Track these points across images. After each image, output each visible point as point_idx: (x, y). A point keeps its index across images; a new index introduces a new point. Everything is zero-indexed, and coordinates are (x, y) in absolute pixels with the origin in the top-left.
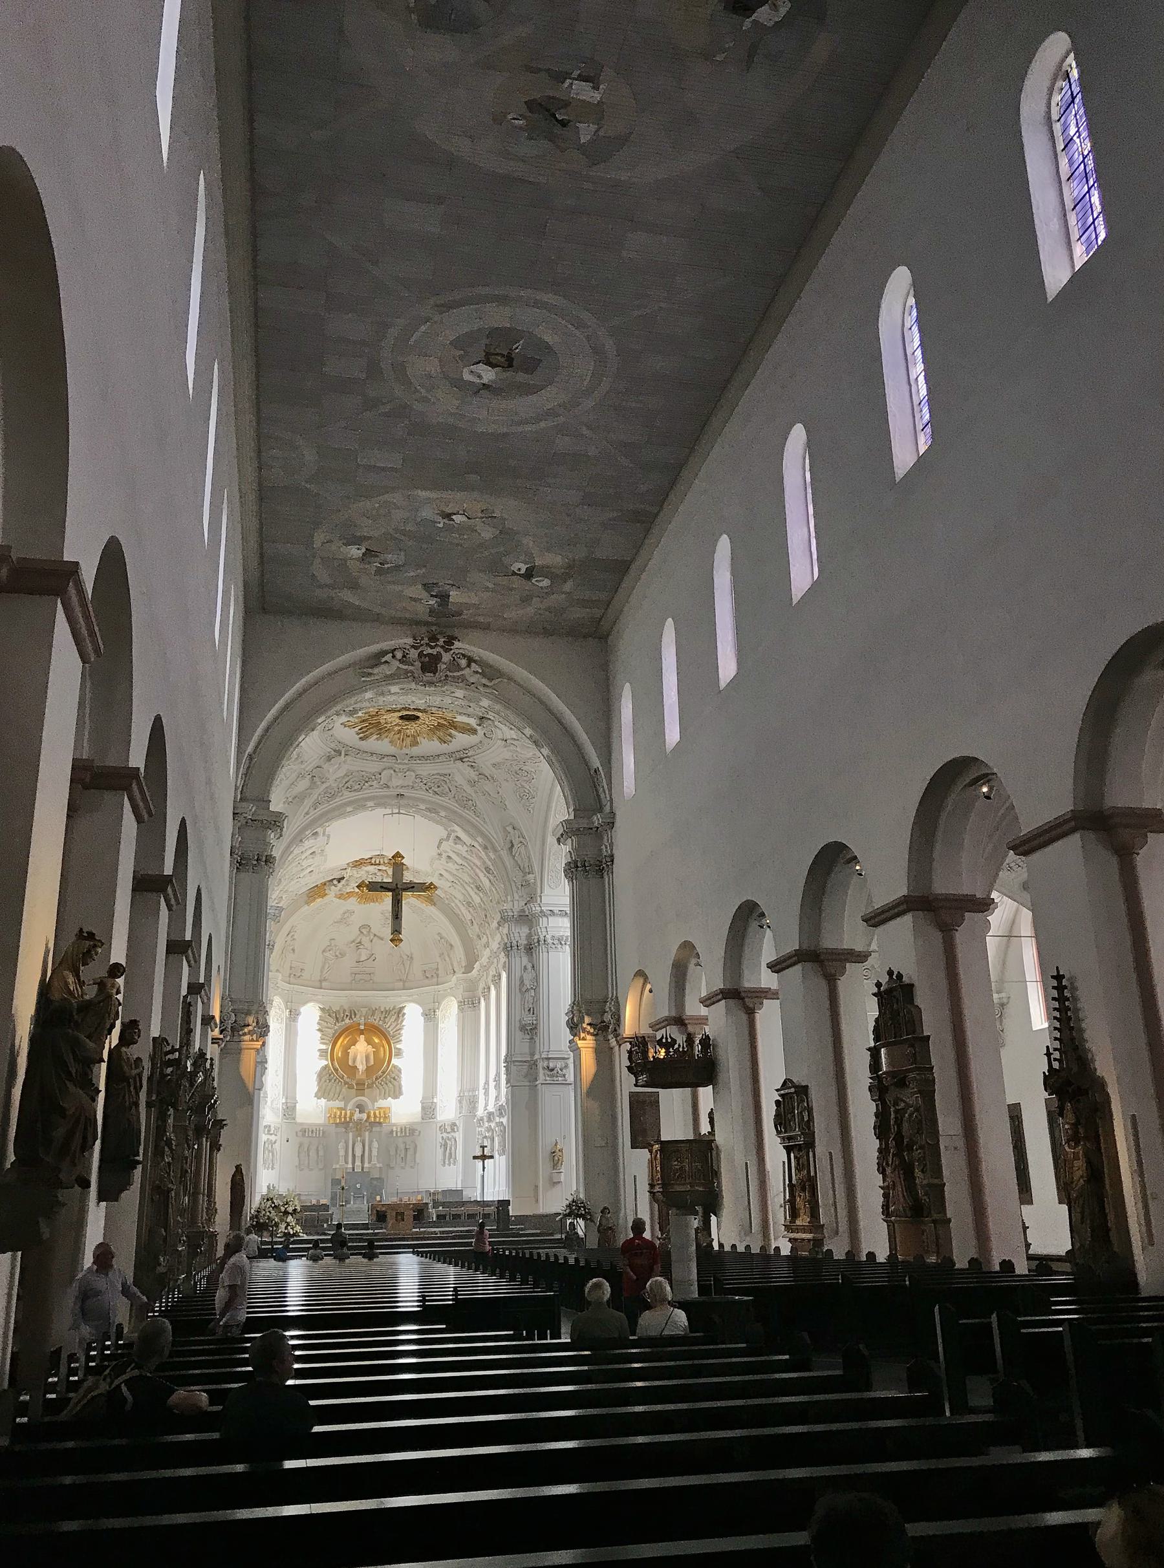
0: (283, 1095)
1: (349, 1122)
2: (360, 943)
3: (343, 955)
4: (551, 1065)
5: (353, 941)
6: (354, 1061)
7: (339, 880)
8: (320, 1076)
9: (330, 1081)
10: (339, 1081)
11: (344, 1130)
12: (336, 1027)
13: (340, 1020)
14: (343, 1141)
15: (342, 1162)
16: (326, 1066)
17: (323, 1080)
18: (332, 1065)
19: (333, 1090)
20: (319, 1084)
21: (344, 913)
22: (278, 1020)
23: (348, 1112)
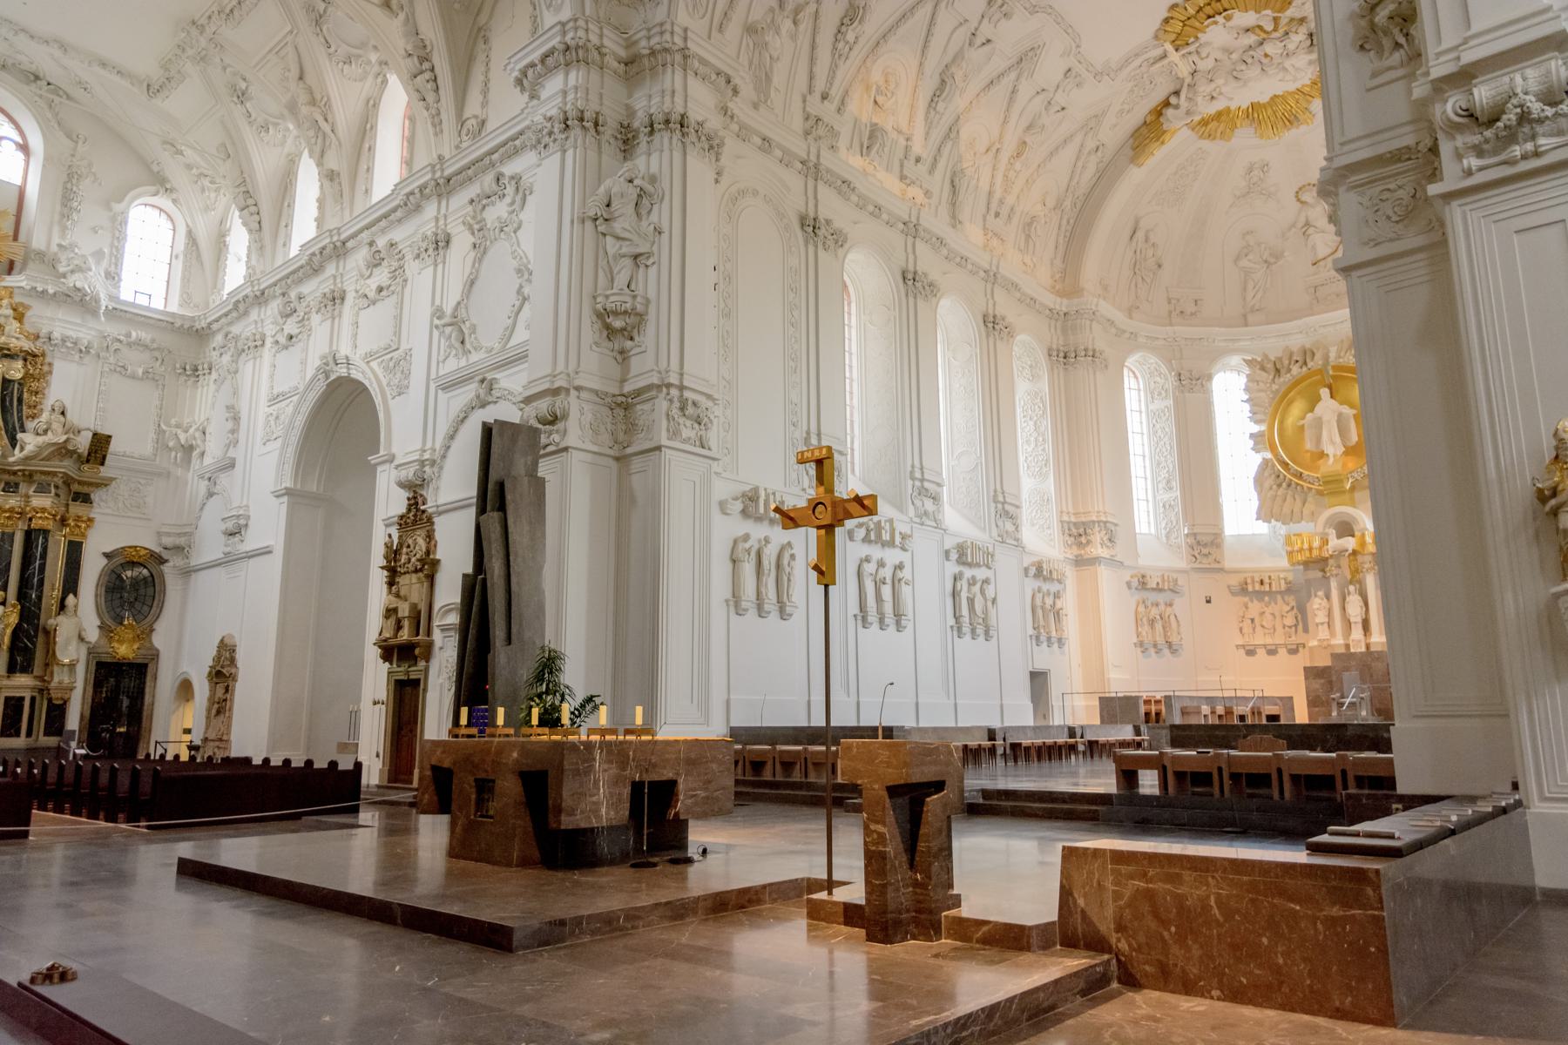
0: (1185, 520)
1: (1325, 560)
2: (1307, 224)
3: (1278, 256)
4: (1483, 94)
5: (1294, 225)
6: (1318, 440)
7: (1177, 93)
8: (1259, 481)
9: (1279, 486)
10: (1297, 484)
11: (1320, 574)
12: (1275, 387)
13: (1283, 371)
14: (1320, 593)
15: (1323, 633)
16: (1265, 462)
17: (1267, 485)
18: (1276, 455)
19: (1289, 499)
20: (1259, 494)
21: (1250, 170)
22: (1160, 394)
23: (1316, 544)
